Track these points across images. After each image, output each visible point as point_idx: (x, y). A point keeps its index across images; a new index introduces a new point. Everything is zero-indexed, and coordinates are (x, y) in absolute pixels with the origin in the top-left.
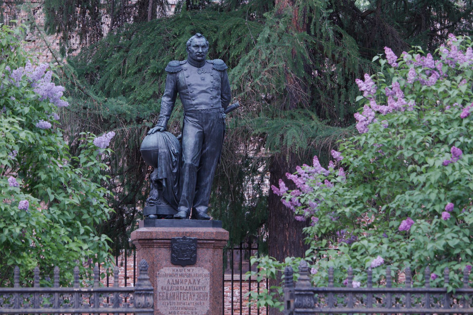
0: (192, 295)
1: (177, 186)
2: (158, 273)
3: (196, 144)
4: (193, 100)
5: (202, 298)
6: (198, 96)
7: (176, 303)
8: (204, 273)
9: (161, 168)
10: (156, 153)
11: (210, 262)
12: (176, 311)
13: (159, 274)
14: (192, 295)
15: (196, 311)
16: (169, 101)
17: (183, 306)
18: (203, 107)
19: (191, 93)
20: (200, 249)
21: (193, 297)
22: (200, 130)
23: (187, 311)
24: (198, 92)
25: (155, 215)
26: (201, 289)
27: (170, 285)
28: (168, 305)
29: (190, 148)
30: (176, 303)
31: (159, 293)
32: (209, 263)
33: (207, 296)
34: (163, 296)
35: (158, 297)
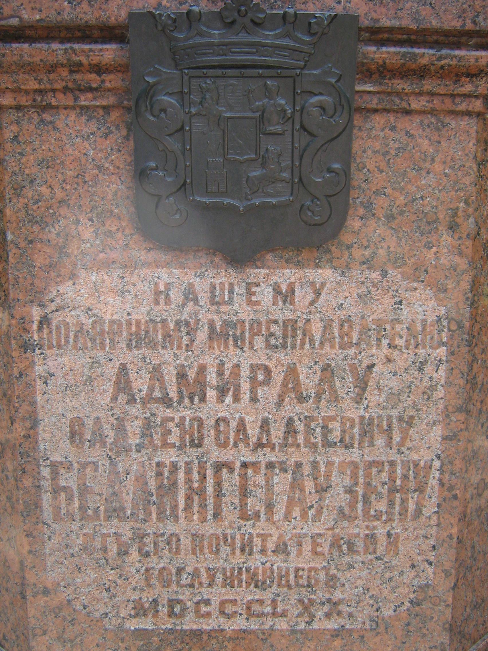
0: (309, 485)
2: (36, 313)
5: (382, 506)
7: (186, 541)
8: (405, 313)
11: (453, 227)
12: (185, 595)
13: (44, 321)
14: (309, 485)
15: (337, 595)
17: (239, 559)
20: (379, 120)
21: (311, 499)
23: (268, 596)
26: (380, 441)
27: (134, 410)
28: (123, 553)
30: (186, 541)
31: (54, 467)
32: (446, 238)
33: (420, 489)
34: (84, 490)
35: (46, 499)
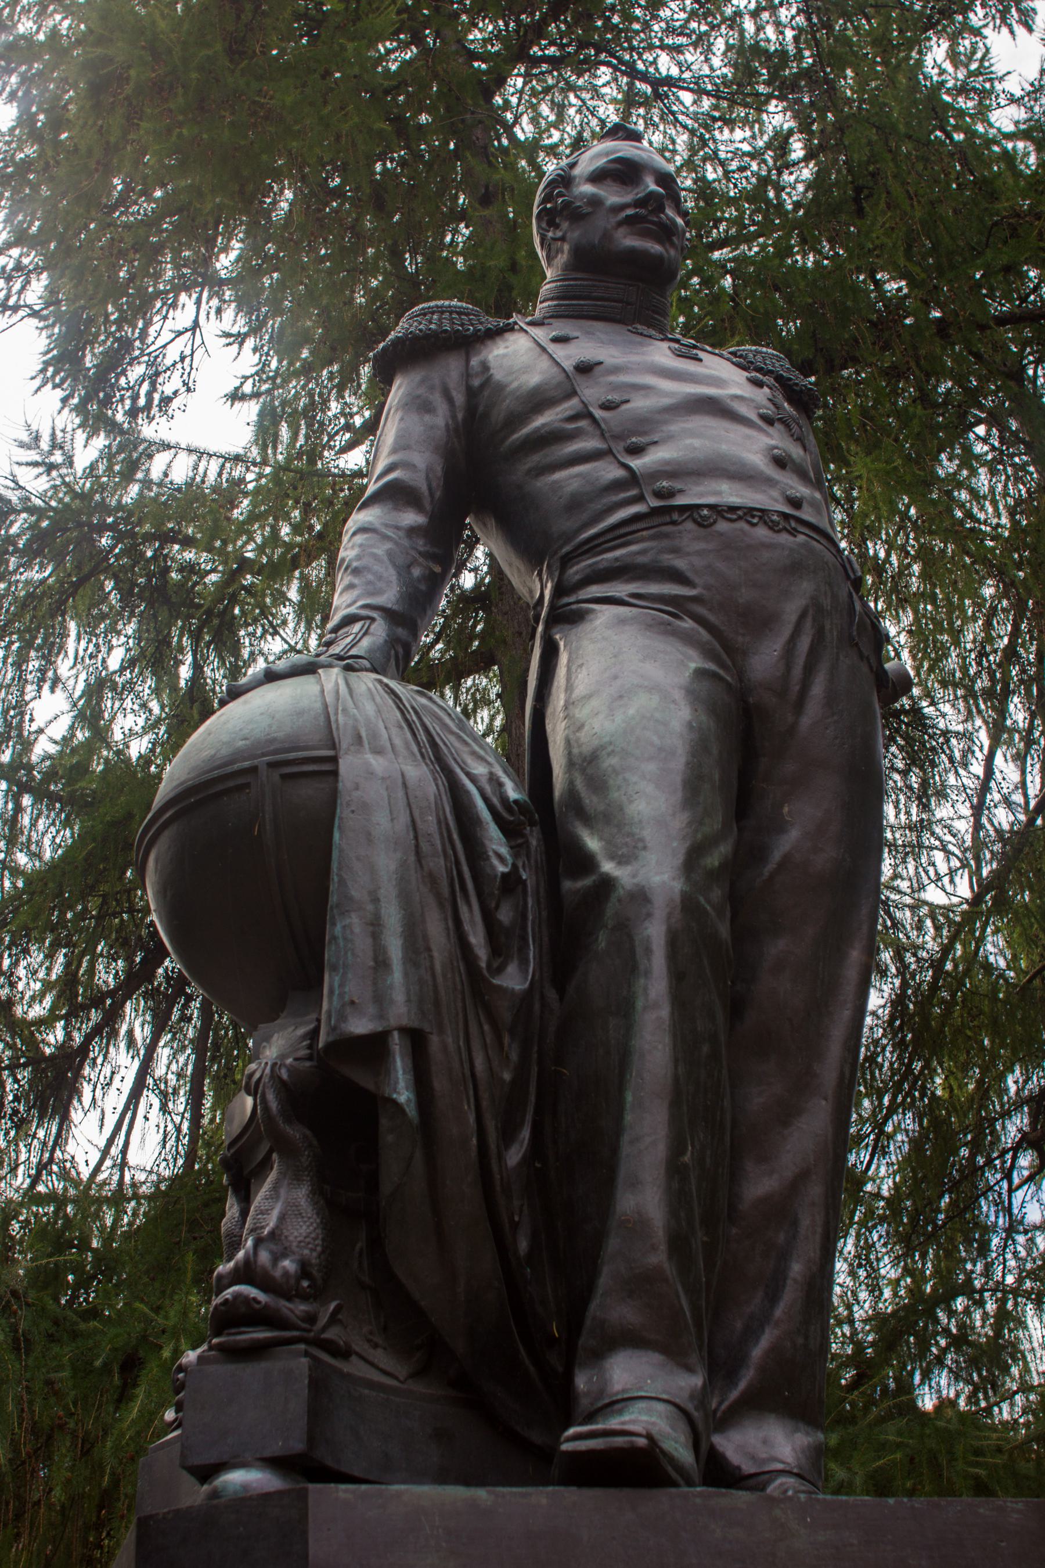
1: (527, 1160)
3: (699, 748)
4: (636, 451)
6: (674, 428)
9: (375, 926)
10: (308, 791)
16: (412, 531)
18: (730, 494)
19: (607, 406)
22: (711, 666)
24: (666, 401)
25: (276, 1463)
29: (651, 767)
